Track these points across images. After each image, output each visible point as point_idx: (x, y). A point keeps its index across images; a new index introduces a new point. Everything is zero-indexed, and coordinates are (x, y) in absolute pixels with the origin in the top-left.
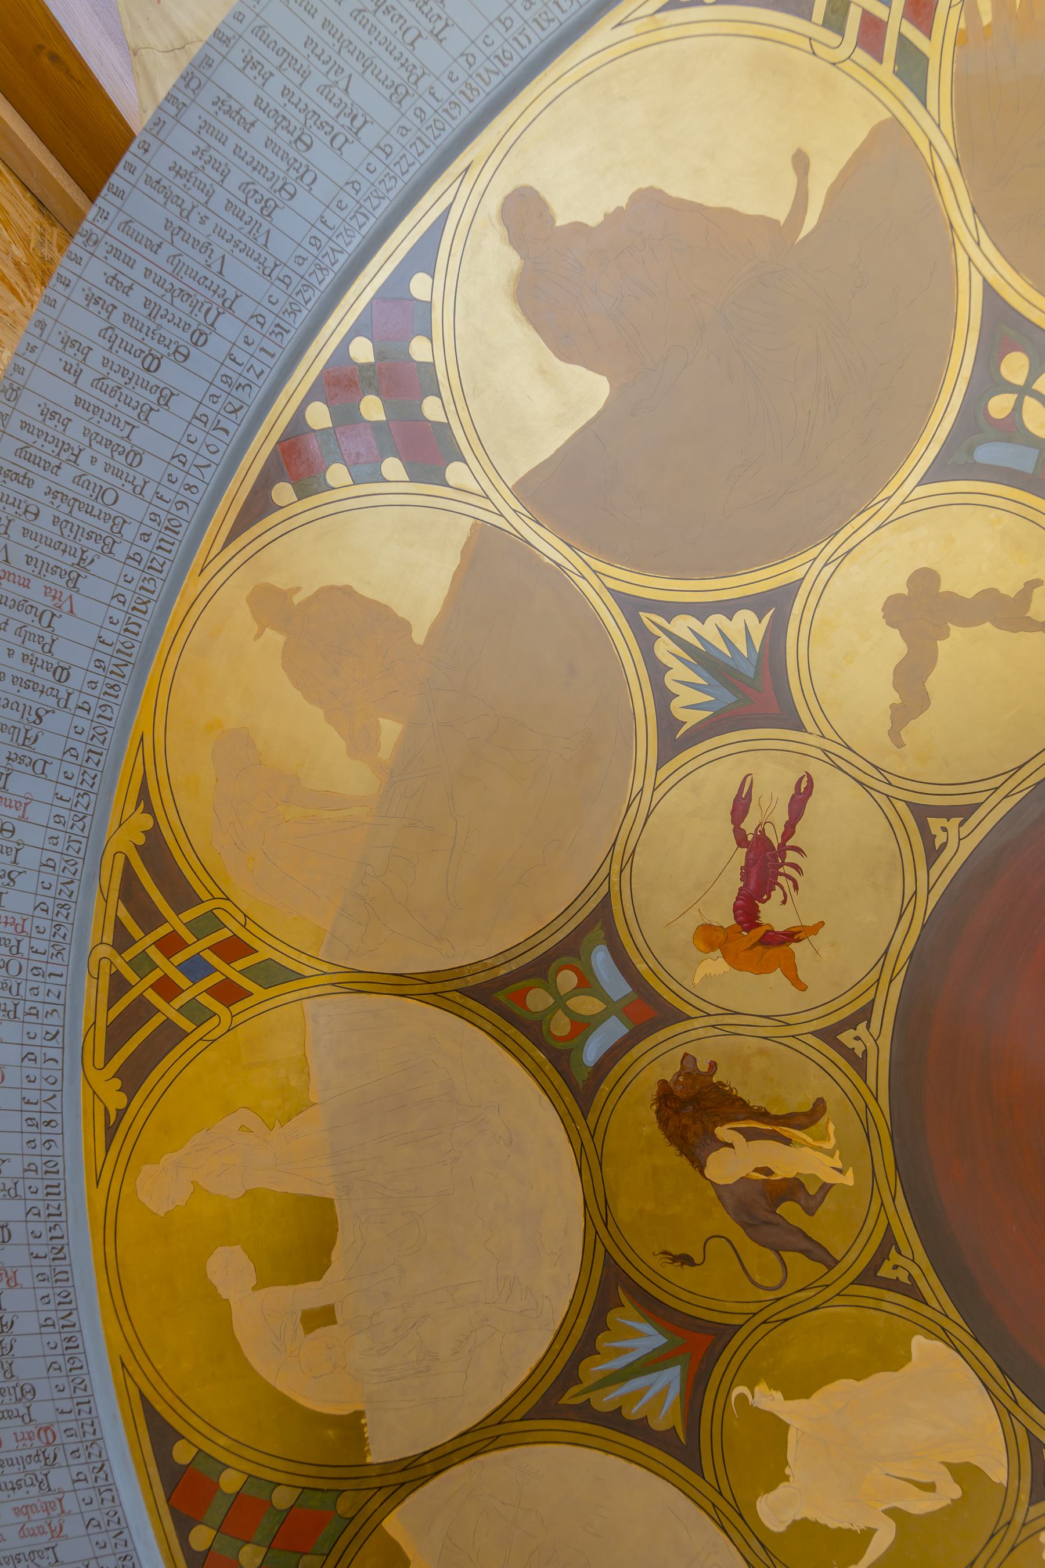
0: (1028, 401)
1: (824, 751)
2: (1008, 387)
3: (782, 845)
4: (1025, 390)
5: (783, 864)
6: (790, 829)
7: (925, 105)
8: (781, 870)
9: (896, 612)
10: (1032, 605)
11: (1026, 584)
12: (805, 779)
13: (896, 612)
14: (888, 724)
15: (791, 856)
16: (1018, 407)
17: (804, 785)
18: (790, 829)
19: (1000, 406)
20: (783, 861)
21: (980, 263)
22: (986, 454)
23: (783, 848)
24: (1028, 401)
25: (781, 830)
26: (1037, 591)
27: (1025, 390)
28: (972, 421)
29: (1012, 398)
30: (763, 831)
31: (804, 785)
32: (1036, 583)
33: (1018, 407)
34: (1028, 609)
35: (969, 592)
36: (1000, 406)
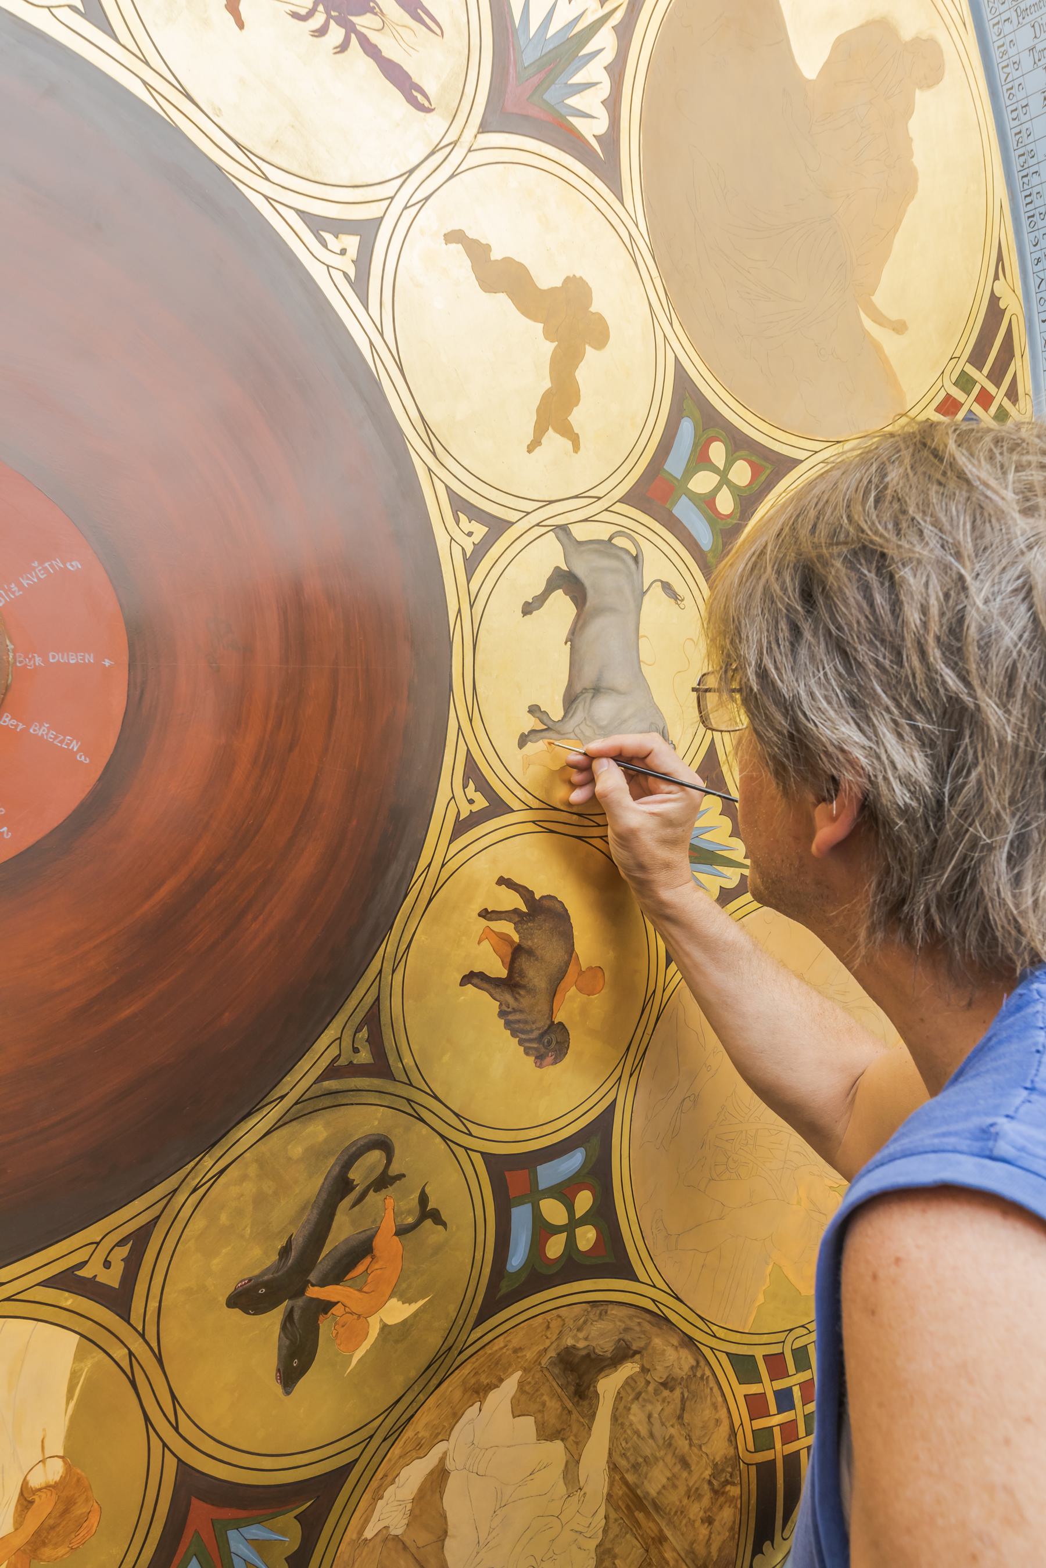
1: (455, 143)
3: (351, 29)
5: (329, 17)
6: (371, 50)
8: (321, 8)
9: (576, 290)
10: (558, 436)
12: (427, 104)
13: (576, 290)
14: (471, 234)
15: (336, 34)
17: (420, 98)
18: (371, 50)
20: (332, 17)
23: (351, 29)
25: (374, 38)
26: (569, 444)
30: (372, 11)
31: (420, 98)
32: (576, 448)
34: (556, 431)
35: (582, 374)
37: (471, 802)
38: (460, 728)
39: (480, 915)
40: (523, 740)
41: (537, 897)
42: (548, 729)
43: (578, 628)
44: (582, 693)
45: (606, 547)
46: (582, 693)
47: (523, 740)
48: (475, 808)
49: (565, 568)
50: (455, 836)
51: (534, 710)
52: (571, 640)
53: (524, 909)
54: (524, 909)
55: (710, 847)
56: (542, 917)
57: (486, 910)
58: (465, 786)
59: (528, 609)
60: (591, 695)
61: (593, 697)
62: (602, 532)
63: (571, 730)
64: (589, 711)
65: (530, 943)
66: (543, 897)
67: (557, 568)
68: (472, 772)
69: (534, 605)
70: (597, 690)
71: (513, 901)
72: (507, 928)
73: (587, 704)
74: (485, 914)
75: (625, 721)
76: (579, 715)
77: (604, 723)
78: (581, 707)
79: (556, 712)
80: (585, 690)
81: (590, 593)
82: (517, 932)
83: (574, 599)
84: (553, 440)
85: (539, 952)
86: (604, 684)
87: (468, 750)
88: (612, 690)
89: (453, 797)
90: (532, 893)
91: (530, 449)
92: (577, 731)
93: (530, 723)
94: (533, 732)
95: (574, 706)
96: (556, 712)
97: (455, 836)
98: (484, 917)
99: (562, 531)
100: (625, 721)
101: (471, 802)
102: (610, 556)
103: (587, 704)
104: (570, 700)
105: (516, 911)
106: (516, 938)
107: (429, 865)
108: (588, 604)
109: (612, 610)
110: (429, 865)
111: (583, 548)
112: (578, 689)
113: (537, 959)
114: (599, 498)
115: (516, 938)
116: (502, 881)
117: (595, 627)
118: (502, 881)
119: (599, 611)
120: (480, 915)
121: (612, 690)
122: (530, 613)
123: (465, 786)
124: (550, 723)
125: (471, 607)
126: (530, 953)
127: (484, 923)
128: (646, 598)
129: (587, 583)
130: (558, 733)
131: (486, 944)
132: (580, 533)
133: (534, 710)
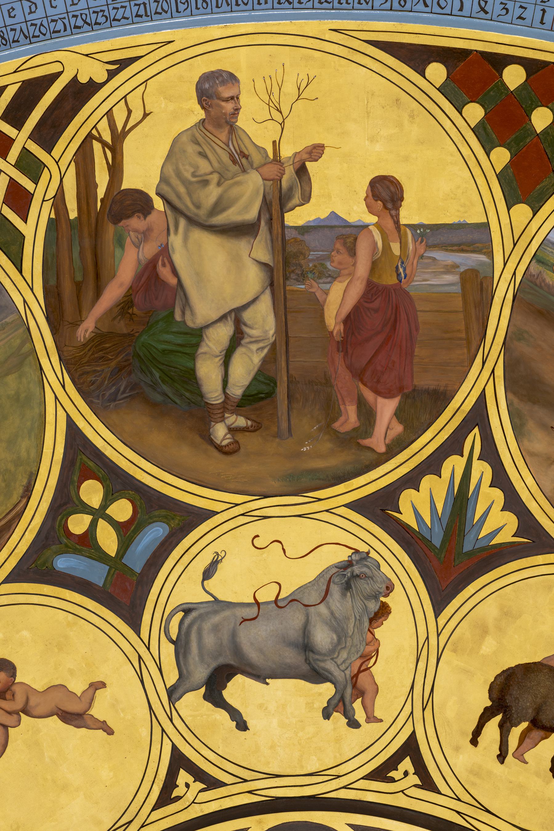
0: (101, 523)
2: (85, 509)
4: (100, 514)
7: (21, 272)
11: (91, 685)
16: (93, 525)
19: (78, 524)
21: (63, 403)
22: (63, 563)
24: (101, 523)
27: (100, 514)
28: (54, 533)
29: (87, 519)
33: (93, 525)
36: (78, 524)
37: (406, 774)
38: (345, 787)
39: (502, 762)
40: (353, 724)
41: (489, 703)
42: (342, 699)
43: (254, 672)
44: (309, 664)
45: (181, 646)
46: (309, 664)
47: (353, 724)
48: (411, 770)
49: (203, 690)
50: (434, 789)
51: (327, 714)
52: (265, 679)
53: (499, 717)
54: (499, 717)
55: (451, 502)
56: (508, 699)
57: (498, 756)
58: (393, 780)
59: (242, 726)
60: (311, 654)
61: (313, 652)
62: (168, 650)
63: (343, 674)
64: (325, 655)
65: (530, 711)
66: (491, 698)
67: (205, 697)
68: (381, 774)
69: (239, 721)
70: (306, 646)
71: (492, 728)
72: (516, 733)
73: (317, 657)
74: (502, 757)
75: (332, 613)
76: (329, 665)
77: (335, 637)
78: (322, 664)
79: (327, 690)
80: (306, 659)
81: (222, 660)
82: (519, 723)
83: (229, 677)
84: (98, 711)
85: (539, 701)
86: (301, 640)
87: (362, 778)
88: (306, 630)
89: (402, 791)
90: (486, 709)
91: (110, 732)
92: (343, 667)
93: (338, 718)
94: (345, 715)
95: (322, 671)
96: (327, 690)
97: (434, 789)
98: (504, 758)
99: (173, 693)
100: (332, 613)
101: (406, 774)
102: (187, 642)
103: (317, 657)
104: (316, 676)
105: (501, 725)
106: (524, 725)
107: (458, 813)
108: (232, 662)
109: (234, 635)
110: (458, 813)
111: (185, 671)
112: (305, 668)
113: (545, 703)
114: (140, 657)
115: (524, 725)
116: (474, 742)
117: (253, 655)
118: (474, 742)
119: (237, 650)
120: (502, 762)
121: (306, 630)
122: (245, 722)
123: (393, 780)
124: (338, 697)
125: (246, 781)
126: (538, 710)
127: (509, 758)
128: (221, 597)
129: (214, 665)
130: (345, 687)
131: (527, 756)
132: (172, 677)
133: (327, 714)
